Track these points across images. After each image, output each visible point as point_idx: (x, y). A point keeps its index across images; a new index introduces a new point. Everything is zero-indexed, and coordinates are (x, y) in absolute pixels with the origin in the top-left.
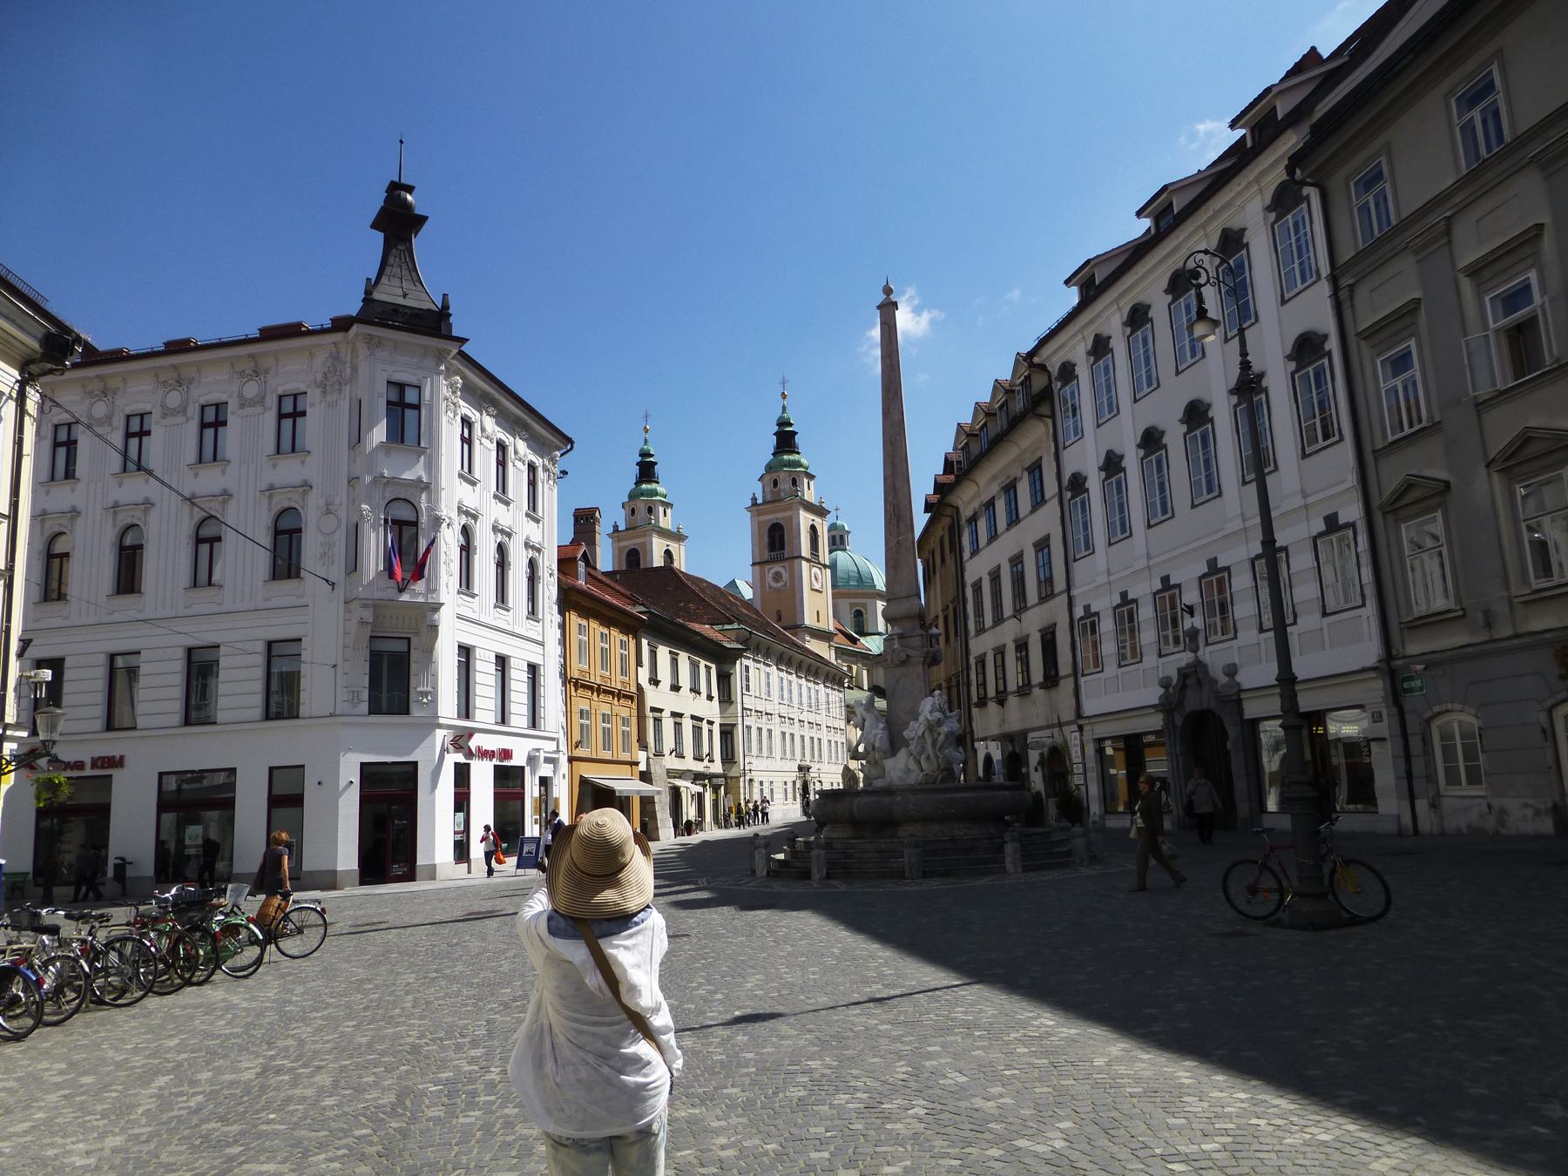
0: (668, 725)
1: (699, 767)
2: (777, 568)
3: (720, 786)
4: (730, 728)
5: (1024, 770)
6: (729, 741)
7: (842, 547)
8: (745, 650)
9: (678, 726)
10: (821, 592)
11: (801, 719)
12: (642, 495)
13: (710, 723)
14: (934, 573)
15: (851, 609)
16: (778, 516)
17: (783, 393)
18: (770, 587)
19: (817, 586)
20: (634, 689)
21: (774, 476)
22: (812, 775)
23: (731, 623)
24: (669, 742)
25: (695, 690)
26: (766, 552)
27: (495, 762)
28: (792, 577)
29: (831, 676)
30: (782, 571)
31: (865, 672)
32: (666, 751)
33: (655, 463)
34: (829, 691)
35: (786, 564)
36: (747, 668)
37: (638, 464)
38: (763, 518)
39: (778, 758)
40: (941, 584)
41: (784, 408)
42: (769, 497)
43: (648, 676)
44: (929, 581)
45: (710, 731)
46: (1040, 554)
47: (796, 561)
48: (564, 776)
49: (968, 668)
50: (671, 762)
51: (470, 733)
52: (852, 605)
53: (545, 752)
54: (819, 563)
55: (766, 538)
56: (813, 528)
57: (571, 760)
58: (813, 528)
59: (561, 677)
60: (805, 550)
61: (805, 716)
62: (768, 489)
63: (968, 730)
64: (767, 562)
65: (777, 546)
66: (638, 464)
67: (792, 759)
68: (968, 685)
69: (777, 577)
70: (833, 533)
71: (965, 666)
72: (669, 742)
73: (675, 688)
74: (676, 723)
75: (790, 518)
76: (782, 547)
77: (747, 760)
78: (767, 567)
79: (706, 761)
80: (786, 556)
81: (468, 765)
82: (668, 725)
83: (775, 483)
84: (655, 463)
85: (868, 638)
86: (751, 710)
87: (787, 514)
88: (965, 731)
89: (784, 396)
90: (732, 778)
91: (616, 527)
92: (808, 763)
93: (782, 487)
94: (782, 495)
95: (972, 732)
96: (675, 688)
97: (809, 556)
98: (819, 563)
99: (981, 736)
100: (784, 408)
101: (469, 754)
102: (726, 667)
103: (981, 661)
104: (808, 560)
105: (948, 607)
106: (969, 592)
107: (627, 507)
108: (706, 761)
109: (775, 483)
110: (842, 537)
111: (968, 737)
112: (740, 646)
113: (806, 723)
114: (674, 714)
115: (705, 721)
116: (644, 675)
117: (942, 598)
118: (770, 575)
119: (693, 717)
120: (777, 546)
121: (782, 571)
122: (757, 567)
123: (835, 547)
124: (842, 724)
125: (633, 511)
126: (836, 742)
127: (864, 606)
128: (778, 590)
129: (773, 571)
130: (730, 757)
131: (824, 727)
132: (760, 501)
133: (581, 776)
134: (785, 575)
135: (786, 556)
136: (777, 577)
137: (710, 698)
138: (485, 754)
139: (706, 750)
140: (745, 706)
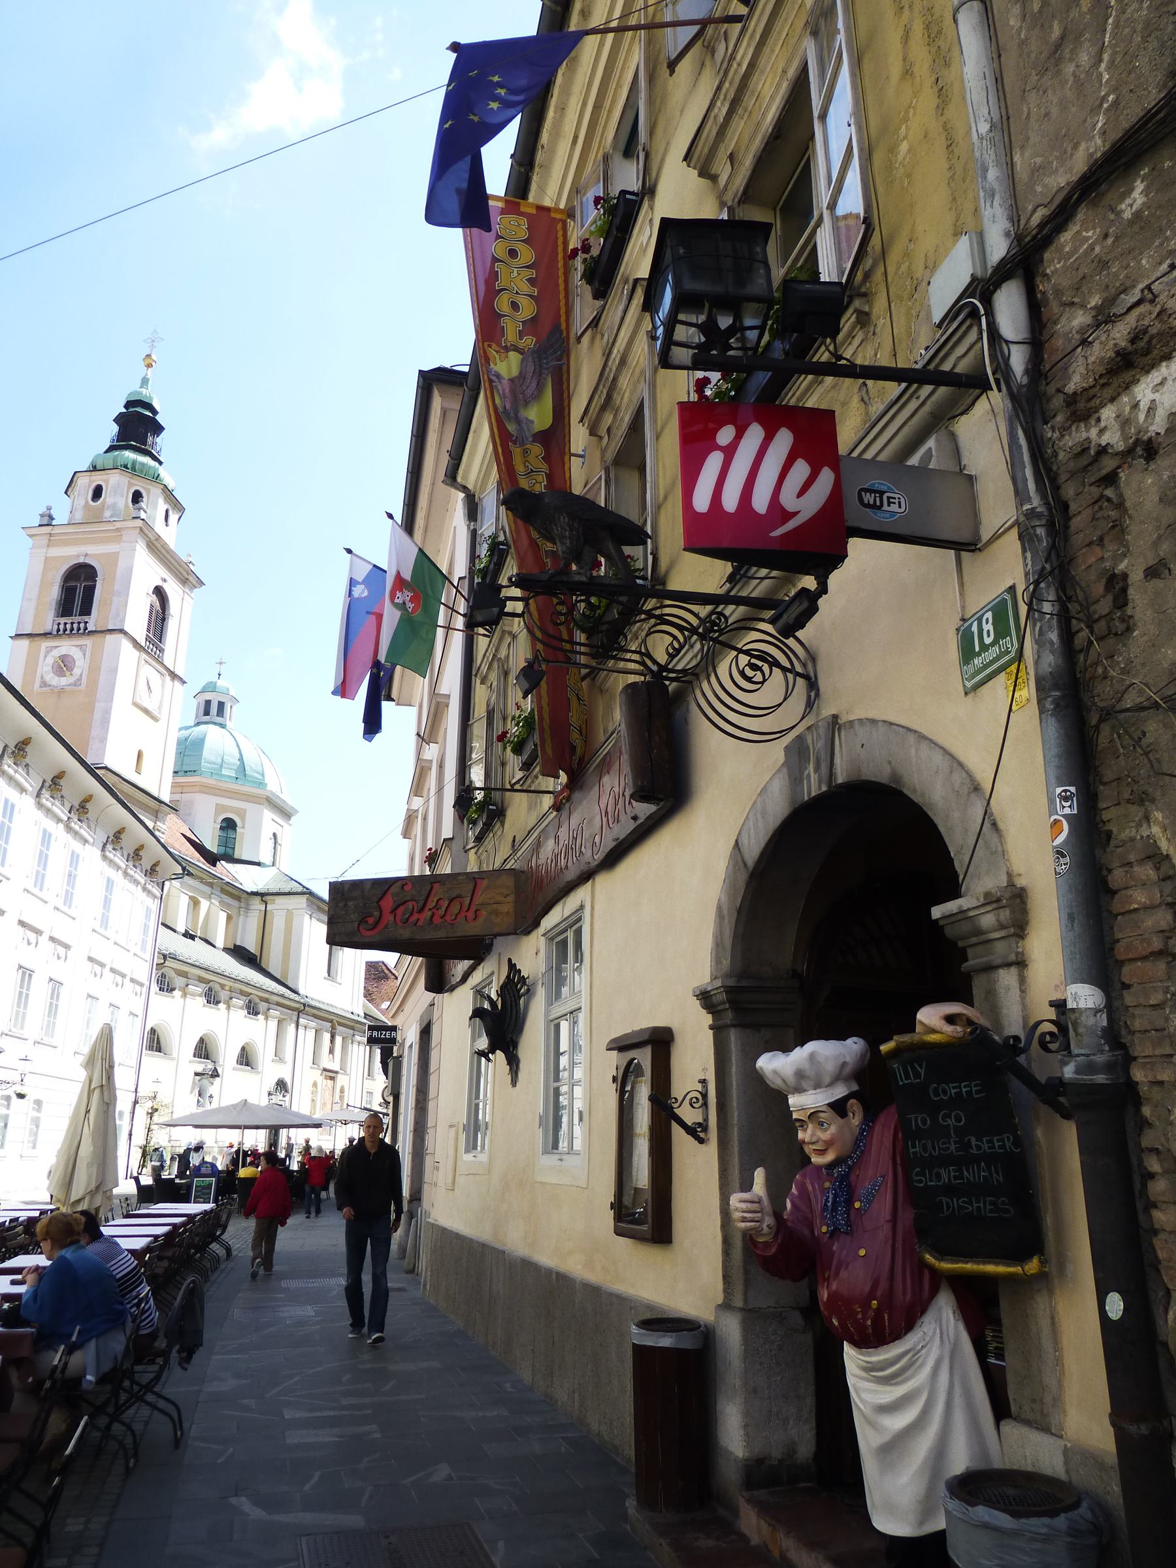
2: (67, 647)
7: (219, 720)
10: (155, 719)
15: (217, 814)
17: (149, 356)
18: (44, 684)
21: (98, 479)
28: (94, 669)
29: (129, 844)
30: (75, 653)
31: (223, 916)
34: (117, 876)
35: (88, 642)
38: (55, 552)
41: (145, 382)
47: (109, 638)
52: (219, 808)
54: (162, 664)
55: (55, 592)
56: (159, 592)
62: (81, 502)
64: (46, 635)
69: (64, 665)
70: (208, 696)
75: (114, 558)
76: (86, 610)
78: (45, 644)
80: (91, 627)
83: (98, 493)
87: (111, 548)
100: (145, 382)
109: (98, 493)
110: (221, 705)
118: (50, 660)
121: (75, 653)
122: (25, 643)
123: (207, 718)
127: (242, 813)
128: (61, 691)
134: (81, 664)
135: (91, 627)
136: (64, 665)
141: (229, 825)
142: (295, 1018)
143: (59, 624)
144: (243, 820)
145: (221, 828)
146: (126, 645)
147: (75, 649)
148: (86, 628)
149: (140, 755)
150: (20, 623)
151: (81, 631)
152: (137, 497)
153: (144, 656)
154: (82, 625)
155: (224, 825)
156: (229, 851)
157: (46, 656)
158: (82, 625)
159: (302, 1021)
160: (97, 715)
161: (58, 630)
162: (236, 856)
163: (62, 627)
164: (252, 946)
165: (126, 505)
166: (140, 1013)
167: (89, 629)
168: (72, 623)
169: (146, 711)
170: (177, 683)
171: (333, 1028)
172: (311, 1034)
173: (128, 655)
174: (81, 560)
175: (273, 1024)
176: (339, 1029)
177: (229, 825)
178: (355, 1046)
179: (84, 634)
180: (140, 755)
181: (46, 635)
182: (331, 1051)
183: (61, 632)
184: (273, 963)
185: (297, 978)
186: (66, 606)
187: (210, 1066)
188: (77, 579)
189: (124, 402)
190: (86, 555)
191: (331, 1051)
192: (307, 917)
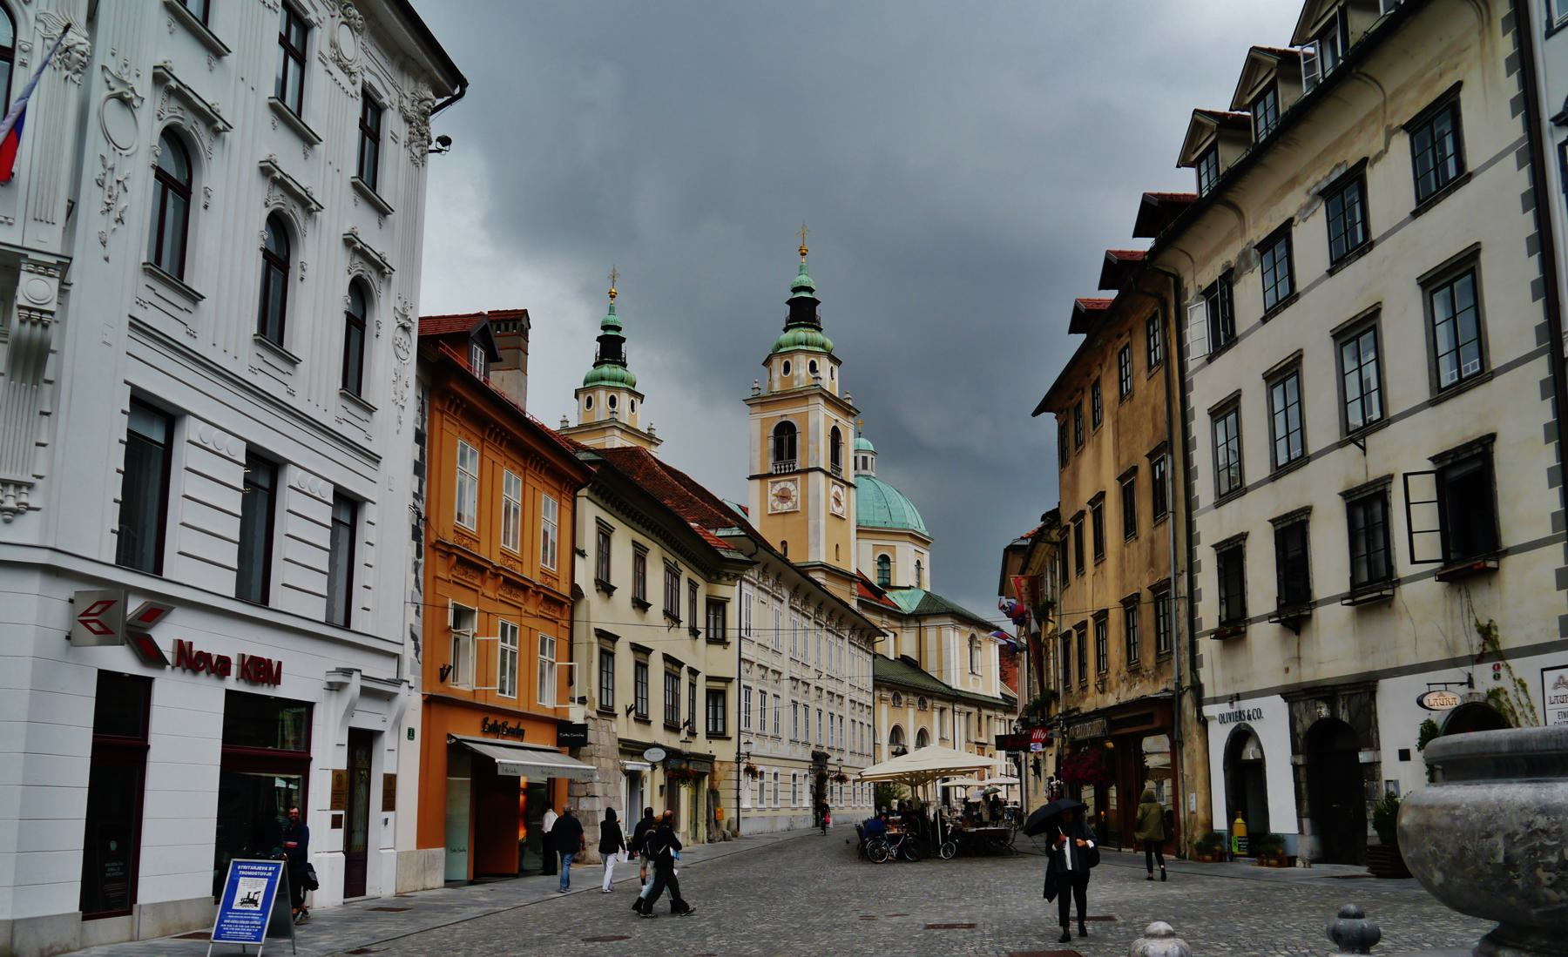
0: (624, 662)
1: (673, 741)
3: (706, 774)
4: (720, 685)
5: (1364, 757)
6: (720, 703)
8: (750, 564)
9: (641, 668)
11: (818, 685)
12: (603, 379)
13: (693, 672)
14: (1097, 423)
15: (874, 553)
16: (789, 412)
18: (773, 508)
19: (838, 511)
20: (565, 589)
22: (830, 768)
23: (729, 526)
24: (624, 696)
25: (672, 616)
26: (771, 460)
27: (233, 683)
28: (805, 497)
32: (620, 709)
33: (623, 340)
35: (799, 477)
36: (748, 597)
37: (599, 339)
39: (786, 740)
40: (1117, 433)
43: (593, 575)
44: (1079, 443)
45: (692, 686)
46: (1278, 392)
47: (811, 475)
48: (411, 733)
49: (1192, 568)
50: (626, 728)
51: (158, 608)
53: (364, 678)
54: (842, 481)
55: (771, 443)
56: (835, 434)
57: (430, 702)
58: (835, 434)
59: (416, 534)
60: (824, 462)
61: (822, 683)
63: (1187, 683)
64: (770, 475)
65: (786, 455)
66: (599, 339)
67: (807, 744)
68: (1192, 597)
71: (1183, 563)
72: (624, 696)
73: (641, 604)
74: (637, 664)
76: (793, 455)
77: (743, 740)
79: (684, 734)
80: (798, 467)
81: (148, 682)
82: (624, 662)
84: (623, 340)
85: (896, 593)
86: (752, 663)
87: (804, 409)
88: (1178, 685)
90: (722, 762)
92: (825, 750)
93: (796, 373)
94: (796, 383)
95: (1197, 688)
96: (641, 604)
97: (829, 470)
98: (842, 481)
99: (1220, 693)
101: (150, 654)
102: (723, 591)
103: (1232, 555)
104: (827, 474)
105: (1134, 470)
106: (1200, 427)
107: (581, 396)
108: (684, 734)
111: (1187, 701)
112: (742, 557)
113: (824, 692)
114: (636, 648)
115: (684, 670)
116: (585, 573)
117: (1118, 458)
119: (667, 658)
120: (786, 455)
121: (790, 486)
122: (757, 482)
124: (869, 701)
125: (589, 401)
126: (861, 723)
129: (778, 487)
130: (720, 729)
131: (847, 700)
133: (450, 736)
136: (784, 497)
137: (694, 632)
138: (192, 661)
139: (684, 715)
140: (743, 656)
141: (884, 560)
142: (951, 707)
144: (894, 554)
145: (879, 564)
146: (821, 476)
147: (789, 483)
148: (794, 468)
149: (837, 546)
150: (751, 468)
151: (791, 470)
152: (813, 367)
153: (831, 480)
155: (880, 560)
156: (887, 581)
159: (956, 708)
160: (811, 528)
161: (776, 470)
162: (892, 584)
164: (914, 656)
165: (807, 373)
166: (872, 725)
167: (797, 469)
169: (837, 516)
170: (852, 489)
171: (979, 710)
172: (963, 718)
175: (936, 714)
176: (985, 712)
177: (884, 560)
178: (998, 723)
180: (837, 546)
181: (770, 475)
182: (980, 730)
183: (779, 472)
184: (931, 667)
185: (950, 677)
187: (901, 748)
189: (790, 288)
190: (786, 415)
191: (980, 730)
192: (952, 632)
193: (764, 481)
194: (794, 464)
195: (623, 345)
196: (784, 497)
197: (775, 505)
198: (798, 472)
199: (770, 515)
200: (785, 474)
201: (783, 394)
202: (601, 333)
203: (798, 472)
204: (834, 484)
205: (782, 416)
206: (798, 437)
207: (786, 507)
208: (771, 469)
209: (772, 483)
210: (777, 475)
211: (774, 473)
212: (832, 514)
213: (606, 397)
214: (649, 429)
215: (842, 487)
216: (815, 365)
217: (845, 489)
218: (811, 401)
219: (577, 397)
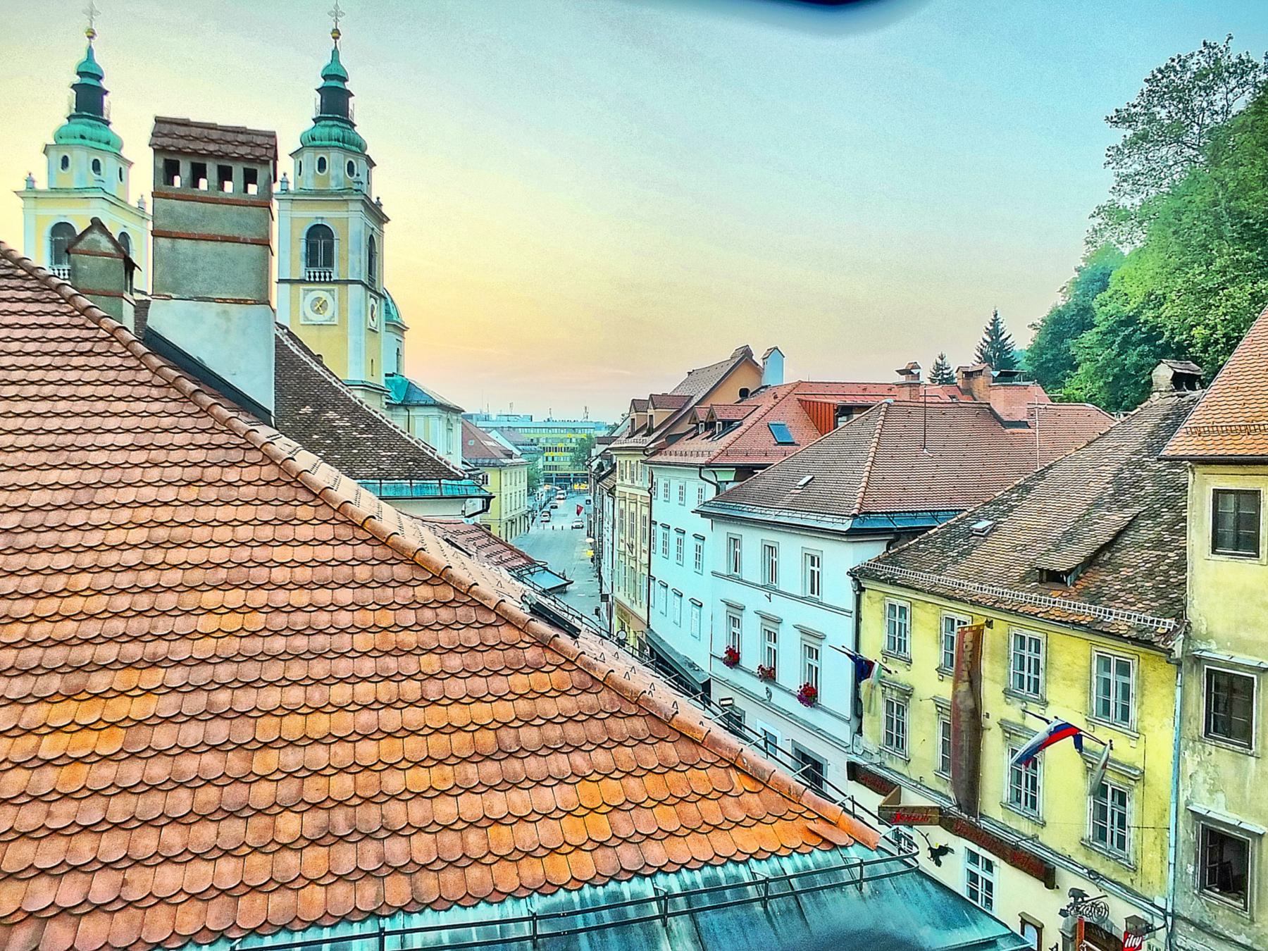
2: (320, 292)
19: (373, 325)
26: (303, 265)
28: (342, 310)
35: (336, 287)
42: (310, 184)
54: (375, 292)
55: (302, 247)
64: (302, 281)
65: (321, 261)
76: (329, 262)
80: (334, 277)
83: (322, 164)
87: (345, 215)
89: (336, 34)
91: (30, 181)
98: (375, 292)
109: (322, 164)
120: (321, 261)
121: (324, 295)
122: (287, 286)
132: (291, 187)
143: (309, 272)
148: (330, 277)
153: (369, 293)
154: (327, 274)
157: (304, 298)
158: (327, 274)
161: (310, 277)
163: (312, 274)
168: (320, 272)
173: (356, 291)
174: (320, 223)
179: (330, 282)
181: (302, 281)
183: (312, 279)
186: (311, 259)
188: (317, 236)
190: (322, 218)
193: (295, 286)
194: (330, 273)
195: (105, 98)
196: (320, 306)
197: (308, 315)
198: (336, 282)
199: (302, 325)
200: (320, 282)
201: (319, 193)
202: (77, 80)
203: (336, 282)
204: (371, 296)
205: (317, 218)
206: (336, 243)
207: (317, 319)
208: (301, 273)
209: (304, 290)
210: (310, 282)
211: (307, 279)
212: (370, 329)
213: (88, 158)
214: (139, 203)
215: (375, 299)
216: (353, 166)
217: (378, 301)
218: (352, 206)
219: (45, 152)
